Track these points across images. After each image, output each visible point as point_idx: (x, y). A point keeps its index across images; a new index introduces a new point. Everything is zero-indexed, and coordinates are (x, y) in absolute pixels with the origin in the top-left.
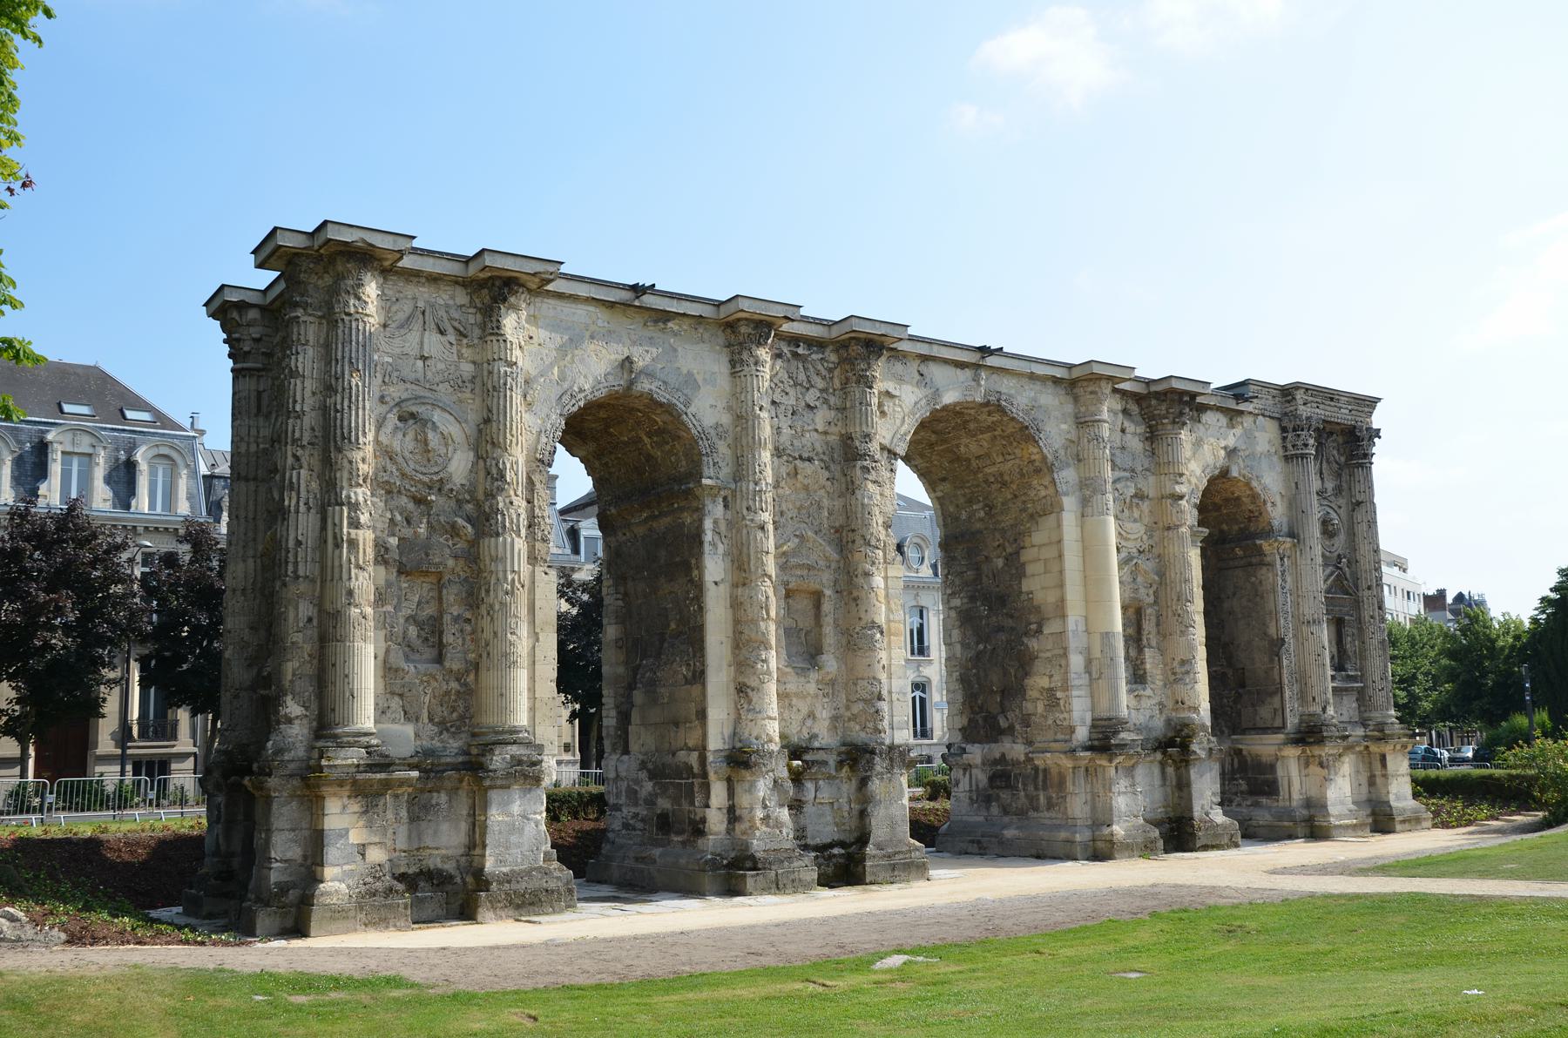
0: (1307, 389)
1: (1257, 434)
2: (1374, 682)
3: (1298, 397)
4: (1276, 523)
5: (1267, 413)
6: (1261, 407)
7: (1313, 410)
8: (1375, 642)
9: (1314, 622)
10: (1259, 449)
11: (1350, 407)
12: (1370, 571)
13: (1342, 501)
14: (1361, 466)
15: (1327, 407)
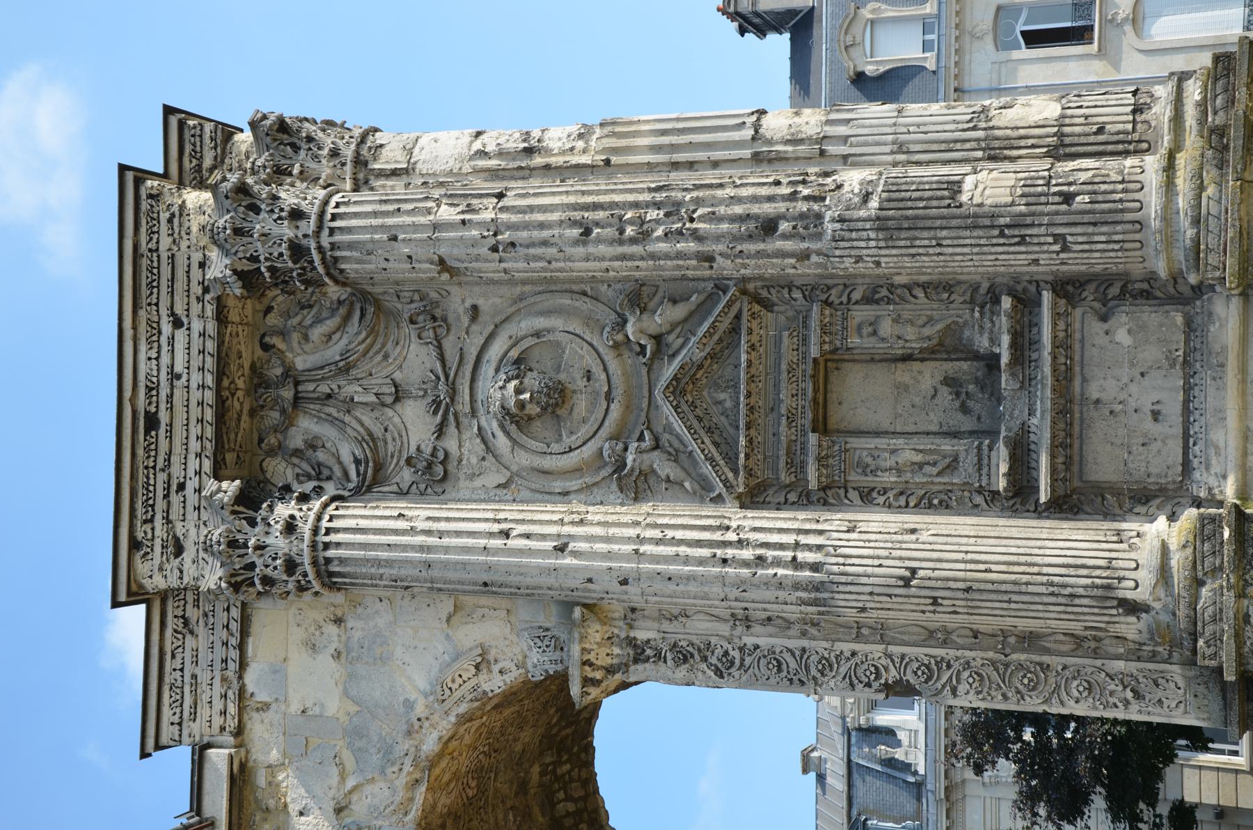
0: (135, 545)
1: (295, 708)
2: (1036, 262)
3: (159, 582)
4: (539, 663)
5: (232, 666)
6: (218, 688)
7: (192, 515)
8: (890, 260)
9: (815, 602)
10: (334, 705)
11: (166, 328)
12: (653, 256)
13: (457, 303)
14: (332, 265)
15: (178, 448)
